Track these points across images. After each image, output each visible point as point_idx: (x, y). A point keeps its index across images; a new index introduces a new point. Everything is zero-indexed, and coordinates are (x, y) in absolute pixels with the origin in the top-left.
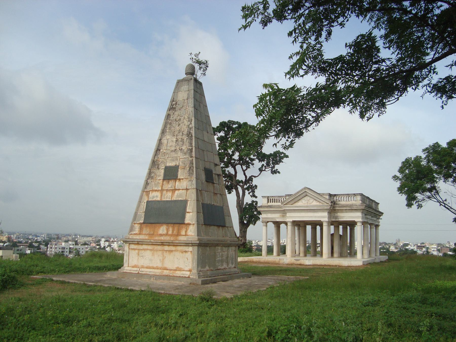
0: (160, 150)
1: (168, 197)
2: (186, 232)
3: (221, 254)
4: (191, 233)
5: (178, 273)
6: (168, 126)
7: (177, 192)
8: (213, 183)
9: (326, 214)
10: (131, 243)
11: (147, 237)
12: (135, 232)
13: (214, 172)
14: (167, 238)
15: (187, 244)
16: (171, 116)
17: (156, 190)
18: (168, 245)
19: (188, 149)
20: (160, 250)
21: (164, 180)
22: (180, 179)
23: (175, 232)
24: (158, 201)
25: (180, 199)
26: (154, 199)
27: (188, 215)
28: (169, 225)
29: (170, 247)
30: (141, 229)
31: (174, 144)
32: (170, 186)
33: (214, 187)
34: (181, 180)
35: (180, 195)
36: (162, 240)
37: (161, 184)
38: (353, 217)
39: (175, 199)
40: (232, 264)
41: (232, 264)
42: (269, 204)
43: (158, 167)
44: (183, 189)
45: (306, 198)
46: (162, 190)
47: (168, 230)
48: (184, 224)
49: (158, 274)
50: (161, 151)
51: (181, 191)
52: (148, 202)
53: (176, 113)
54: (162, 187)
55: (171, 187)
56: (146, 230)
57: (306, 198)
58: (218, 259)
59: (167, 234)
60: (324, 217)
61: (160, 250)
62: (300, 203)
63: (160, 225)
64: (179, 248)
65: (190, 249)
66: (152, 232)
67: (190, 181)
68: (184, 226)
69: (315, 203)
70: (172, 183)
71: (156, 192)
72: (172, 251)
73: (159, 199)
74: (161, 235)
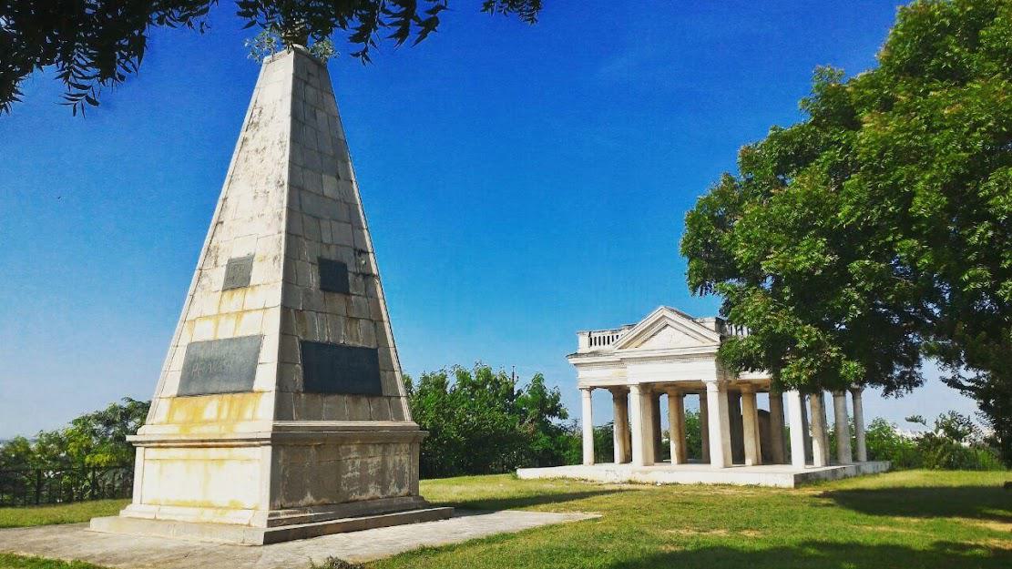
1: (228, 330)
3: (358, 462)
4: (259, 414)
5: (231, 517)
7: (246, 316)
8: (348, 294)
10: (148, 445)
13: (351, 268)
15: (251, 442)
16: (250, 142)
33: (348, 302)
40: (400, 487)
41: (400, 487)
42: (594, 348)
44: (257, 310)
46: (219, 315)
47: (220, 409)
48: (252, 392)
49: (190, 519)
53: (259, 135)
58: (349, 475)
59: (217, 421)
70: (238, 295)
74: (207, 422)
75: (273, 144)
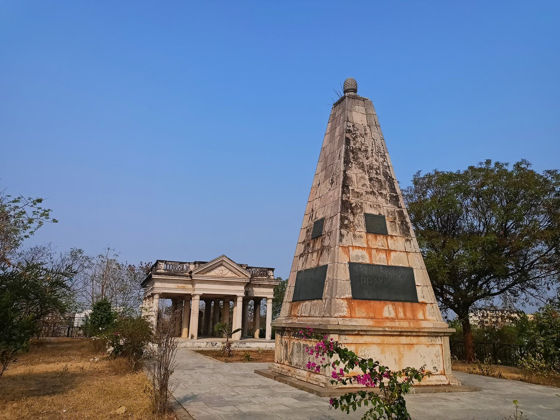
0: (348, 187)
1: (380, 259)
6: (351, 155)
9: (242, 288)
11: (370, 323)
12: (341, 314)
14: (405, 325)
15: (435, 334)
16: (352, 143)
17: (359, 247)
19: (391, 197)
21: (368, 232)
23: (409, 315)
24: (368, 265)
25: (401, 265)
26: (360, 261)
27: (418, 289)
28: (397, 303)
29: (409, 338)
30: (350, 307)
31: (368, 183)
32: (380, 244)
34: (395, 238)
36: (398, 328)
38: (264, 293)
43: (352, 212)
50: (350, 188)
51: (398, 253)
52: (350, 263)
54: (368, 244)
56: (361, 310)
57: (219, 268)
62: (212, 273)
63: (382, 302)
65: (438, 341)
66: (372, 315)
67: (407, 240)
69: (230, 274)
71: (360, 250)
73: (368, 261)
74: (387, 318)
75: (372, 150)
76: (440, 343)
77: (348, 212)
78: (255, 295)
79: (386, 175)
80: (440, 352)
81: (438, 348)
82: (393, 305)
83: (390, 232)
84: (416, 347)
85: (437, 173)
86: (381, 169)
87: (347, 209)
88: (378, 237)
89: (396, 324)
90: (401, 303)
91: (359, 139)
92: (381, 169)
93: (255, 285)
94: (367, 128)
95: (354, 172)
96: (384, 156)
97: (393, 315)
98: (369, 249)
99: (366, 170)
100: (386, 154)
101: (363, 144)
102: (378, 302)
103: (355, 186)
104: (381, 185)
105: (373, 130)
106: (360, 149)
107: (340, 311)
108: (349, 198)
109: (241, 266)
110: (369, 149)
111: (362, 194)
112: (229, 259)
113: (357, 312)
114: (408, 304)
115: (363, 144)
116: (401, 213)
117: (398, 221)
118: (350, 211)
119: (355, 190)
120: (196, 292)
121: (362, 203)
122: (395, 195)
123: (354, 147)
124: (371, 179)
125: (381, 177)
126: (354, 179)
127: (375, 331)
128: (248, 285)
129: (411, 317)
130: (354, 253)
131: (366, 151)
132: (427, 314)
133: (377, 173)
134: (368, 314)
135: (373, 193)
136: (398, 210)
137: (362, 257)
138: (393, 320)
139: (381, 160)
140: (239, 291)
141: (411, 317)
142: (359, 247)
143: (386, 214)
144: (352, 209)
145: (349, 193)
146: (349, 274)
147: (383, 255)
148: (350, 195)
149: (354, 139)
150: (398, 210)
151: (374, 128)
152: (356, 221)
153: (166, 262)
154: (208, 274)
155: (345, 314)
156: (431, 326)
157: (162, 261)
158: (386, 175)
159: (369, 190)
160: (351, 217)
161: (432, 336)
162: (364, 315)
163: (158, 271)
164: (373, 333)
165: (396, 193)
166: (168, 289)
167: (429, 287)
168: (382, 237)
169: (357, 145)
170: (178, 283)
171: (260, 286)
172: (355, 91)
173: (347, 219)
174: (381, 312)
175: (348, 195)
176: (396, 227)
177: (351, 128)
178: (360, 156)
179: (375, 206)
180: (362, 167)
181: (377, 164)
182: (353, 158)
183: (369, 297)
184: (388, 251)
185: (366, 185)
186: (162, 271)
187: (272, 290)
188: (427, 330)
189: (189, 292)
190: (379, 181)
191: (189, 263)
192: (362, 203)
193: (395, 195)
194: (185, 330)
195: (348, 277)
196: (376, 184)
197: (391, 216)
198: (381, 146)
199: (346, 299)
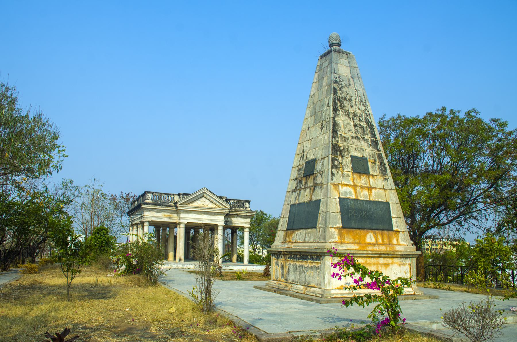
0: (336, 132)
1: (364, 195)
2: (397, 240)
6: (339, 104)
7: (374, 191)
9: (222, 218)
11: (357, 247)
12: (333, 240)
14: (383, 248)
15: (405, 256)
16: (339, 92)
17: (347, 185)
18: (384, 257)
19: (372, 141)
20: (374, 264)
21: (354, 172)
22: (373, 176)
23: (386, 240)
24: (354, 200)
25: (380, 200)
26: (348, 196)
27: (394, 220)
28: (377, 231)
29: (386, 259)
30: (341, 235)
31: (353, 129)
32: (363, 182)
34: (375, 177)
35: (378, 195)
36: (378, 251)
37: (351, 178)
38: (241, 223)
39: (374, 200)
43: (341, 154)
44: (380, 189)
45: (204, 199)
47: (376, 238)
50: (339, 133)
51: (378, 190)
52: (340, 198)
54: (354, 182)
55: (366, 184)
56: (349, 238)
57: (202, 200)
60: (219, 220)
61: (374, 264)
62: (195, 204)
63: (365, 230)
64: (396, 260)
65: (408, 261)
66: (357, 241)
67: (385, 179)
68: (393, 233)
69: (211, 205)
71: (348, 187)
72: (388, 264)
73: (353, 197)
74: (369, 244)
75: (355, 99)
76: (409, 263)
77: (337, 154)
78: (234, 225)
79: (367, 121)
80: (409, 269)
81: (407, 267)
82: (374, 233)
83: (371, 172)
84: (391, 266)
85: (399, 117)
86: (364, 117)
87: (337, 151)
88: (362, 176)
89: (377, 248)
90: (380, 232)
91: (344, 89)
92: (364, 117)
93: (233, 216)
94: (351, 79)
95: (342, 119)
96: (365, 105)
97: (373, 241)
98: (355, 186)
99: (351, 117)
100: (367, 104)
101: (348, 94)
102: (362, 231)
103: (342, 131)
104: (364, 131)
105: (355, 81)
106: (345, 99)
107: (332, 238)
108: (337, 142)
109: (221, 198)
110: (353, 99)
111: (348, 139)
112: (210, 191)
113: (346, 238)
114: (386, 232)
115: (348, 94)
116: (380, 156)
117: (378, 163)
118: (339, 153)
119: (343, 135)
120: (181, 221)
121: (348, 146)
122: (375, 139)
123: (341, 96)
124: (355, 126)
125: (363, 124)
126: (342, 125)
127: (360, 254)
128: (227, 215)
129: (388, 243)
130: (343, 189)
131: (351, 100)
132: (400, 240)
133: (360, 120)
134: (354, 240)
135: (357, 138)
136: (378, 153)
137: (350, 193)
138: (373, 245)
139: (363, 108)
140: (219, 220)
141: (388, 243)
142: (347, 185)
143: (368, 157)
144: (341, 151)
145: (338, 137)
146: (339, 207)
147: (366, 192)
148: (339, 139)
149: (340, 89)
150: (378, 153)
151: (356, 80)
152: (344, 162)
153: (153, 193)
154: (191, 205)
155: (337, 240)
156: (403, 249)
157: (149, 192)
158: (367, 121)
159: (354, 135)
160: (340, 159)
161: (403, 258)
162: (351, 241)
163: (147, 201)
164: (358, 255)
165: (376, 138)
166: (194, 219)
167: (402, 219)
168: (365, 176)
169: (343, 95)
170: (164, 212)
171: (238, 216)
172: (339, 45)
173: (337, 160)
174: (365, 239)
175: (337, 139)
176: (376, 168)
177: (338, 80)
178: (345, 104)
179: (359, 149)
180: (348, 114)
181: (360, 112)
182: (340, 106)
183: (355, 227)
184: (370, 189)
185: (351, 130)
186: (150, 201)
187: (248, 220)
188: (400, 253)
189: (175, 221)
190: (362, 127)
191: (174, 194)
192: (348, 146)
193: (375, 139)
194: (171, 254)
195: (339, 210)
196: (360, 130)
197: (372, 158)
198: (362, 96)
199: (337, 228)
